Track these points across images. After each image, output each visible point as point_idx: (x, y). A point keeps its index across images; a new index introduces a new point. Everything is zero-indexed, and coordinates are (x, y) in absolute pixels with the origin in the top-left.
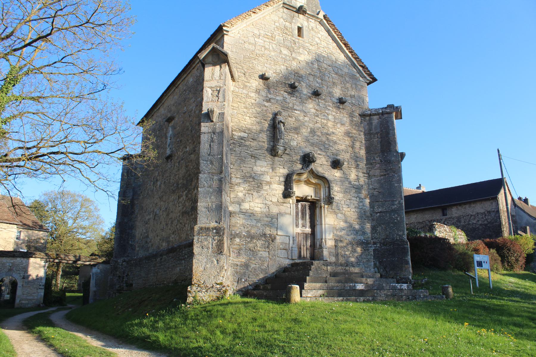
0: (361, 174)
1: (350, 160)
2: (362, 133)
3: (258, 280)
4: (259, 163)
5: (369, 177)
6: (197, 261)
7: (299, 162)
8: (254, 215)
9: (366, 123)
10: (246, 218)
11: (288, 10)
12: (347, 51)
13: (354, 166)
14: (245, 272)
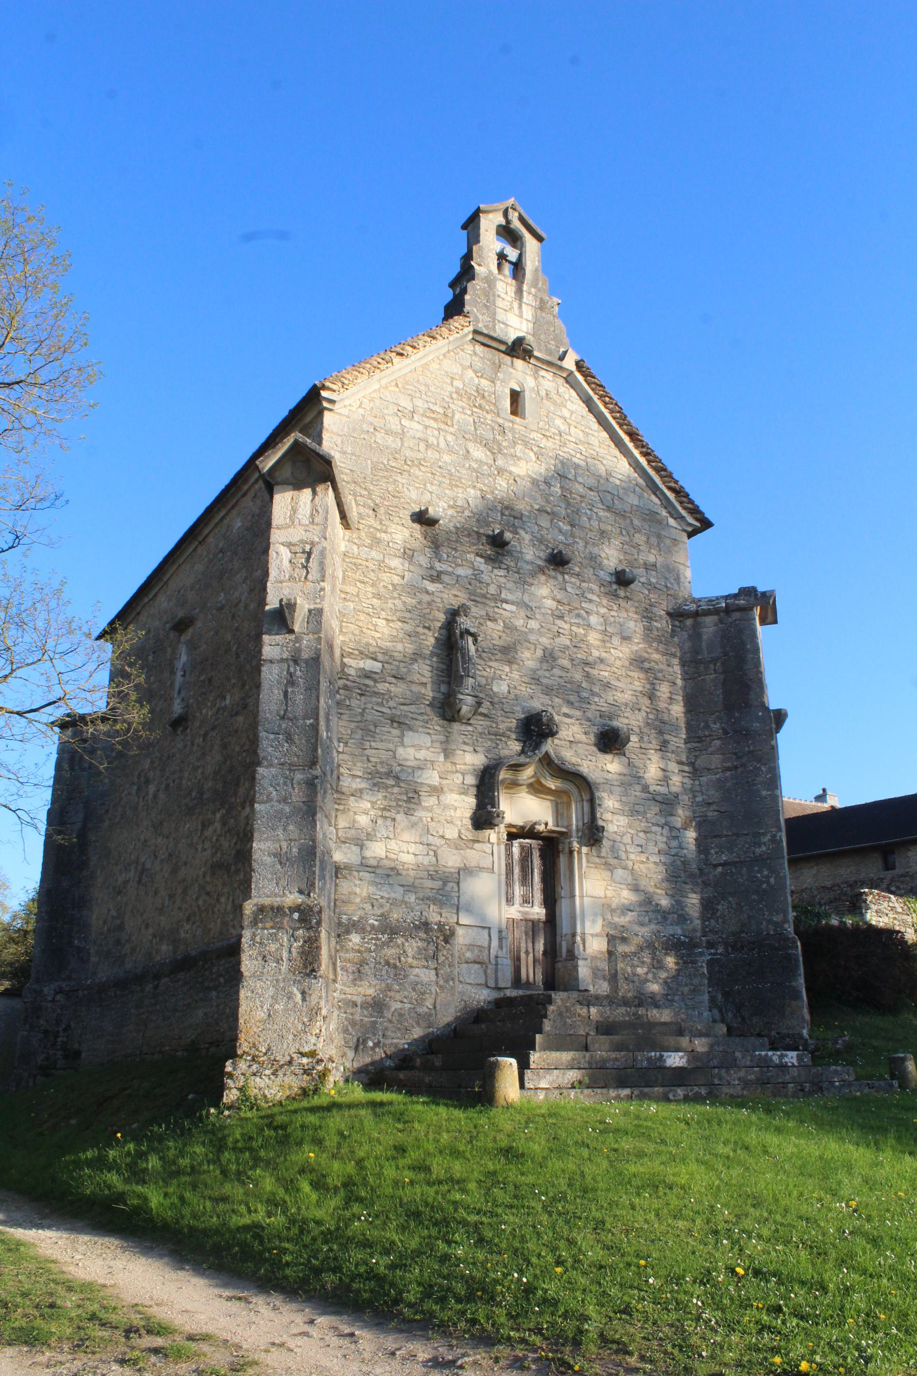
0: (675, 764)
1: (645, 730)
2: (676, 661)
3: (409, 1044)
4: (409, 737)
5: (695, 772)
6: (249, 994)
7: (514, 736)
8: (398, 874)
9: (685, 635)
10: (377, 880)
11: (486, 349)
12: (636, 453)
13: (655, 744)
14: (375, 1023)
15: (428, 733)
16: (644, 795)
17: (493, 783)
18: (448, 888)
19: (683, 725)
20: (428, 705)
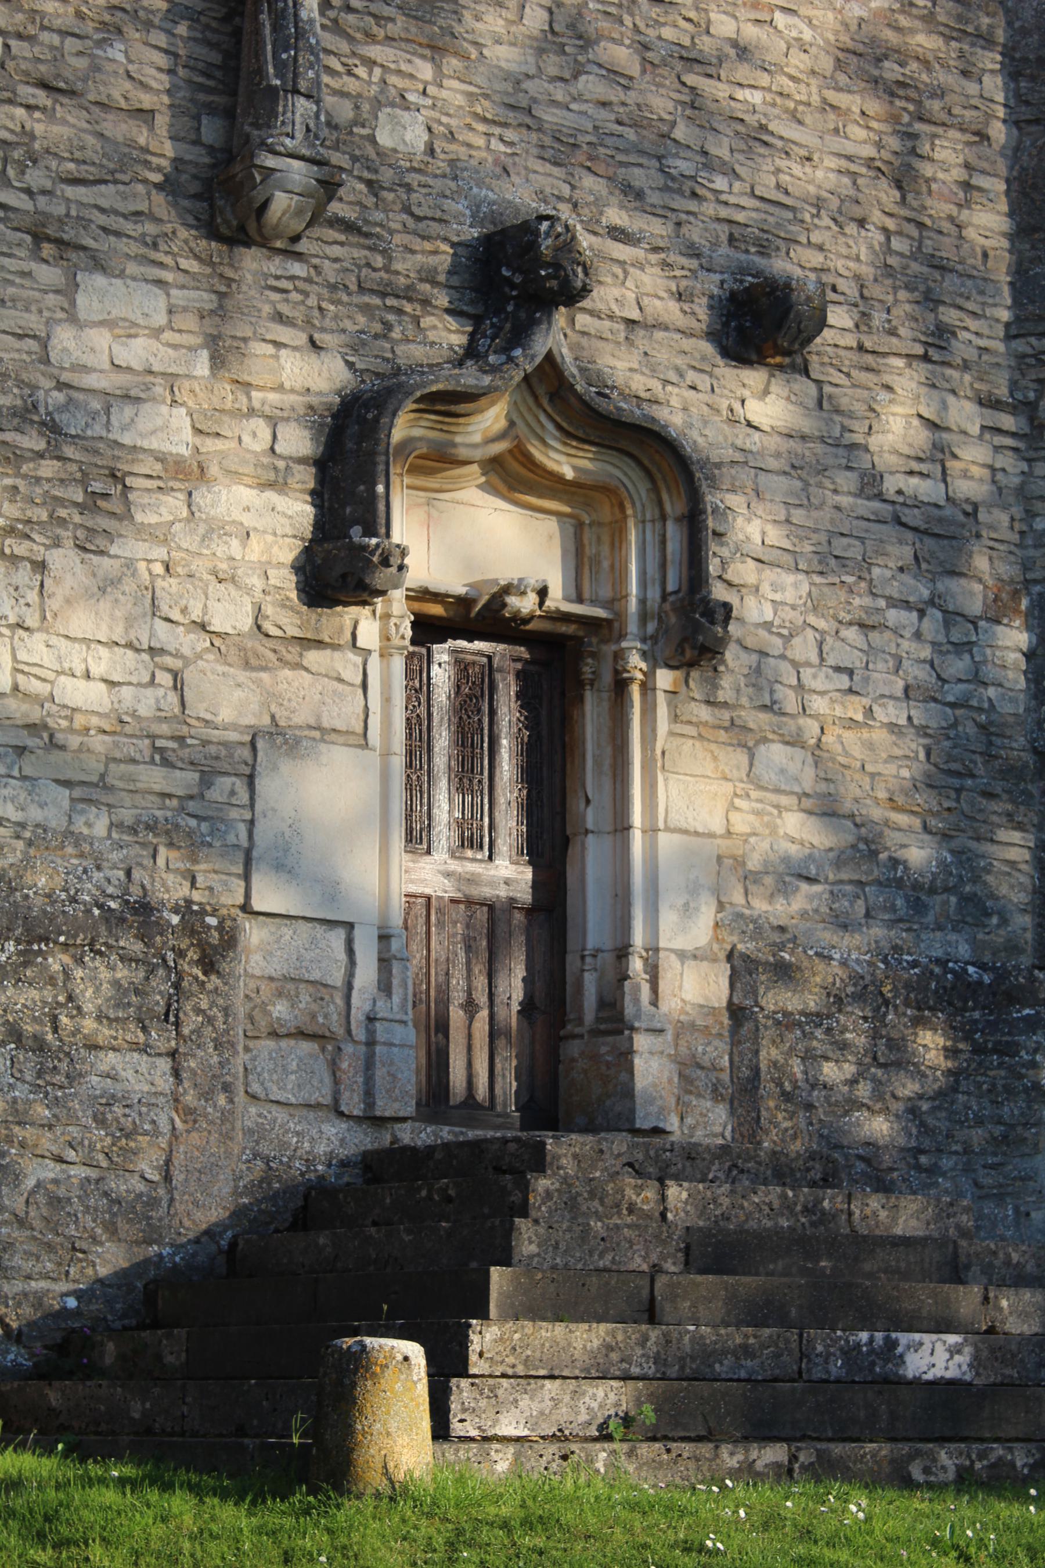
1: (875, 291)
2: (990, 60)
3: (78, 1295)
7: (442, 300)
8: (54, 745)
13: (907, 339)
15: (159, 283)
16: (868, 507)
17: (373, 453)
18: (215, 794)
19: (1004, 278)
20: (159, 187)
